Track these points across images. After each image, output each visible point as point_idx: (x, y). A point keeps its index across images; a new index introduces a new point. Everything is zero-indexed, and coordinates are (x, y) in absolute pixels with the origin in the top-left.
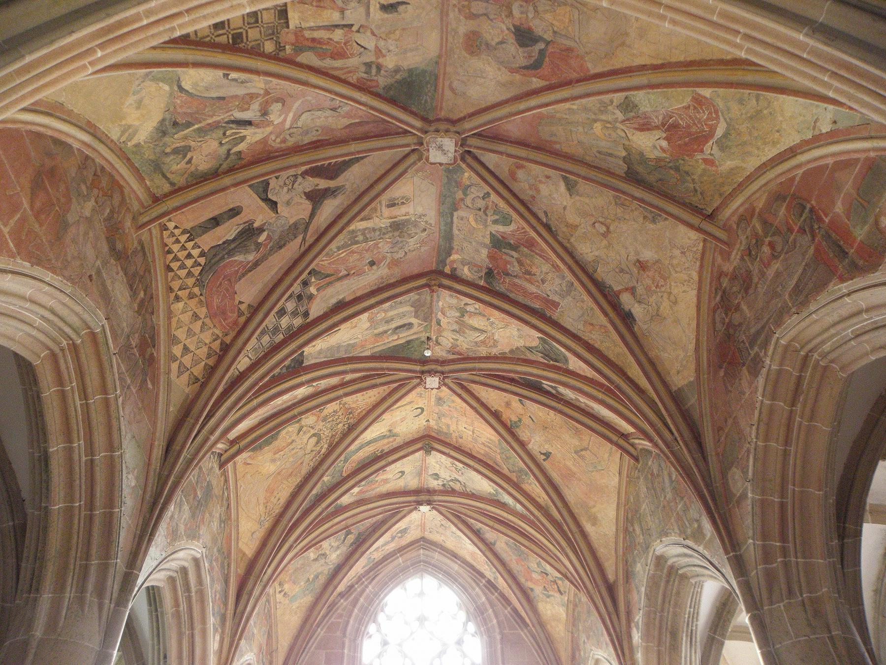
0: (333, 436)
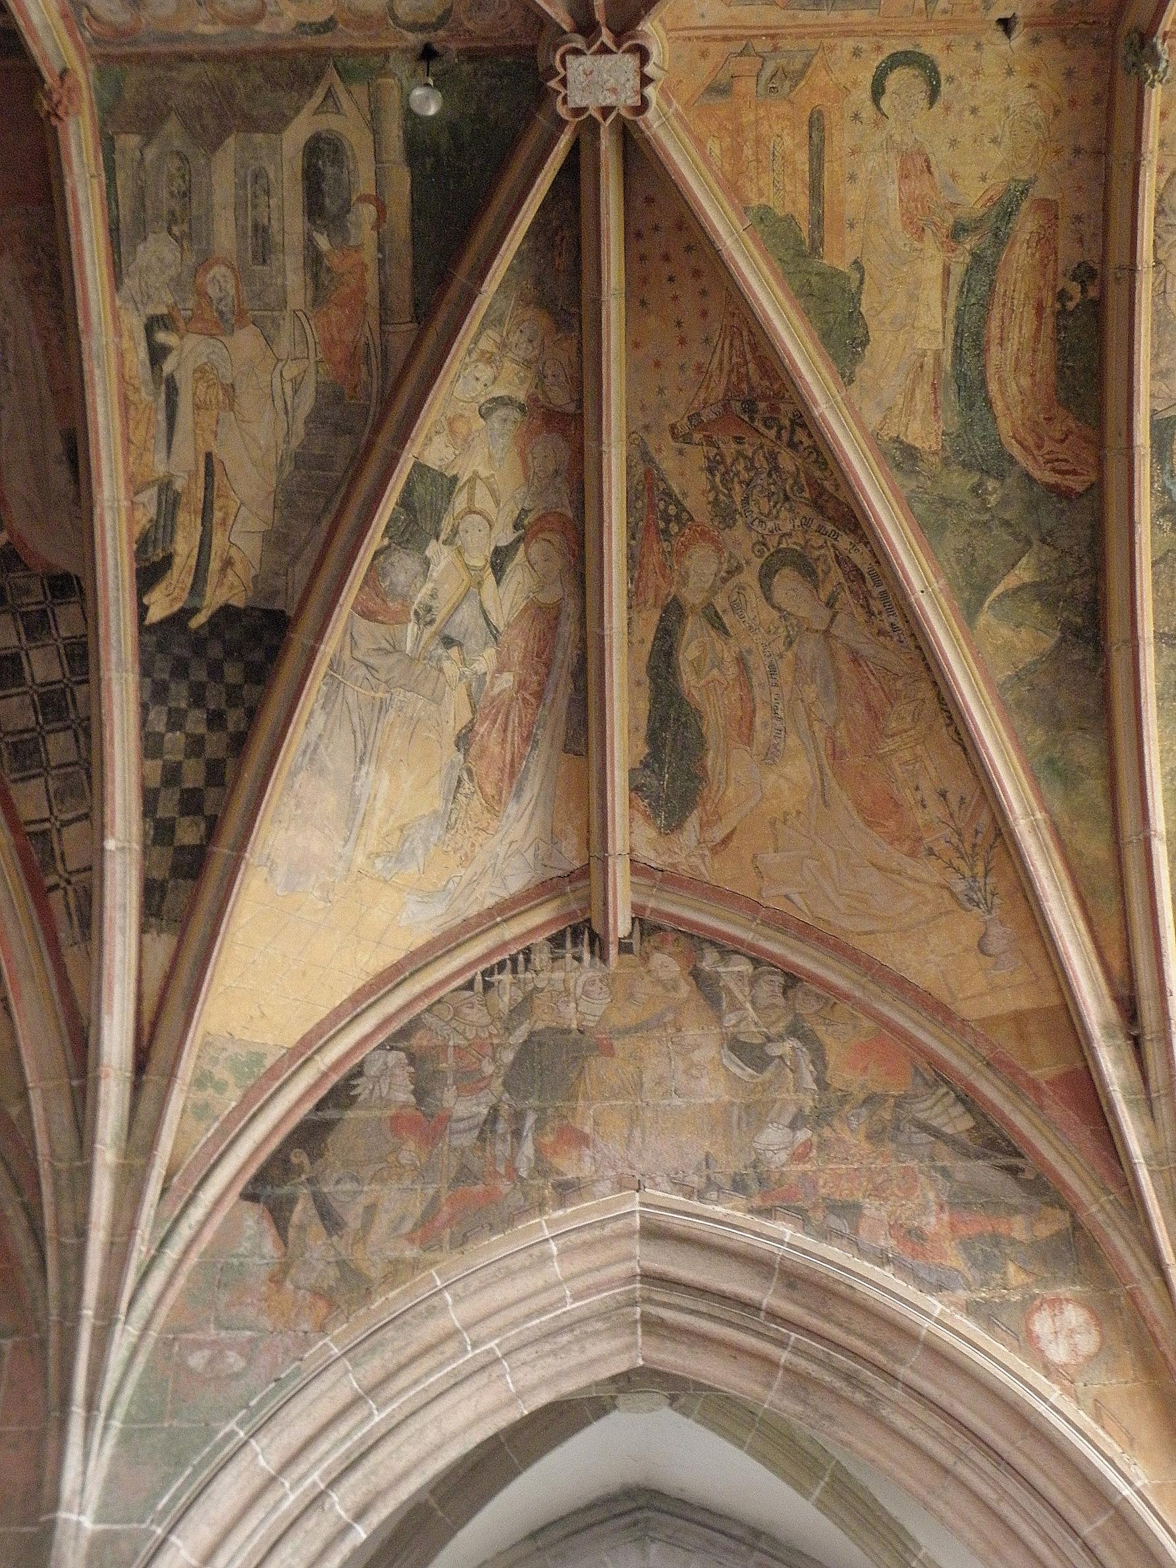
0: (817, 504)
